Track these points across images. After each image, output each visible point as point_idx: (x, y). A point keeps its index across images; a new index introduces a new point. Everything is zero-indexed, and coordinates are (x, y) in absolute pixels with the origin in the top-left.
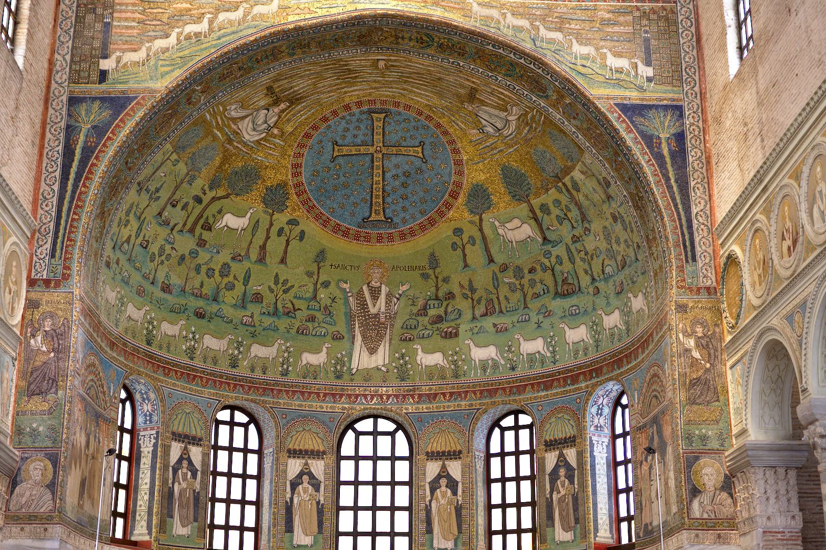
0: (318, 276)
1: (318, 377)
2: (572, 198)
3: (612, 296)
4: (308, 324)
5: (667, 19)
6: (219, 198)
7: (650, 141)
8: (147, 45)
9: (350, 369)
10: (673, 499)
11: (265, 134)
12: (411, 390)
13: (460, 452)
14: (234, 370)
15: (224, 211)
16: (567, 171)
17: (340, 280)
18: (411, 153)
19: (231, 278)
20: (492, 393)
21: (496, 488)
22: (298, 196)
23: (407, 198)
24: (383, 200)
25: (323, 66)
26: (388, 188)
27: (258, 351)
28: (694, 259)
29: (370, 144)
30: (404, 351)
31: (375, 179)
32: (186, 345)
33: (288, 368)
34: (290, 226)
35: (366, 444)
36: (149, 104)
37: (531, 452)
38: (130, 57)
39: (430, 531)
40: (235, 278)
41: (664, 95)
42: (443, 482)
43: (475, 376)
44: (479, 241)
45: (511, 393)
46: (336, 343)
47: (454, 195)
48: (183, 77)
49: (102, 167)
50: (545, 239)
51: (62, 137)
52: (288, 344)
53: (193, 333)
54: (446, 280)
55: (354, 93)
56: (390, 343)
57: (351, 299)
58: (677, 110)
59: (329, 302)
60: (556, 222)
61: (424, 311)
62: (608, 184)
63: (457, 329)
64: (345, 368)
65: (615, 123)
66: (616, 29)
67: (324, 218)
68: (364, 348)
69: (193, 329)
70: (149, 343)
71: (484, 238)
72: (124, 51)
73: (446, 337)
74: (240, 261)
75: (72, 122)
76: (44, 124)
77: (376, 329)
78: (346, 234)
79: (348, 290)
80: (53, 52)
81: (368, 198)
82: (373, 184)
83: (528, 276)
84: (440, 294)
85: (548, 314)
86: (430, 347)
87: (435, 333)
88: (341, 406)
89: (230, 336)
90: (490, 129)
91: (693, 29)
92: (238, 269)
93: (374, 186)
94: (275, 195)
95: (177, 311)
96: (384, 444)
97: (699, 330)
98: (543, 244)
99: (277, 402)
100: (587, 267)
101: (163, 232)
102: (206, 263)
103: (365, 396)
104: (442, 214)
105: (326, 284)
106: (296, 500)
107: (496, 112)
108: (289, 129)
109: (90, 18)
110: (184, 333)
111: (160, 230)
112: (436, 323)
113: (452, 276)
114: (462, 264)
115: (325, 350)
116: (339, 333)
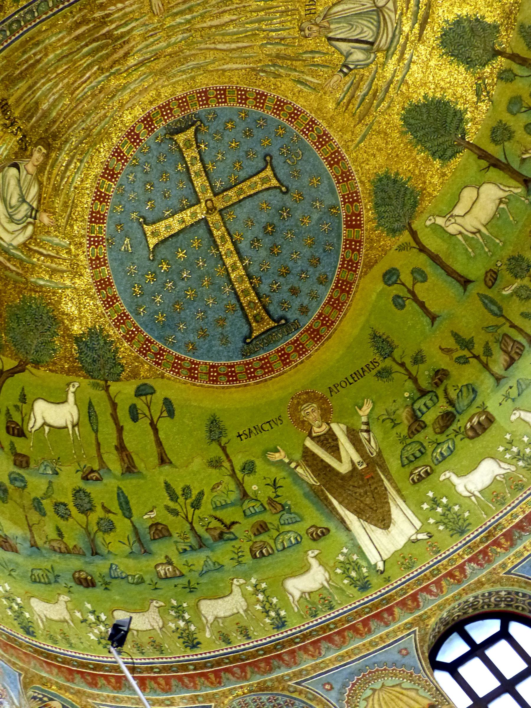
0: (230, 461)
1: (334, 603)
4: (261, 538)
11: (30, 228)
12: (487, 538)
14: (198, 651)
15: (29, 396)
17: (265, 453)
18: (259, 188)
19: (99, 513)
22: (130, 340)
23: (288, 272)
24: (257, 294)
25: (71, 29)
29: (193, 201)
30: (431, 494)
31: (229, 262)
32: (94, 634)
33: (278, 614)
34: (143, 398)
40: (103, 507)
44: (429, 268)
46: (322, 543)
52: (253, 581)
53: (93, 612)
54: (419, 359)
56: (402, 497)
57: (299, 470)
59: (270, 492)
63: (484, 411)
64: (364, 570)
67: (187, 365)
68: (370, 528)
69: (89, 606)
70: (28, 631)
71: (435, 259)
73: (478, 435)
74: (97, 479)
77: (366, 493)
79: (287, 460)
81: (234, 301)
82: (228, 275)
84: (424, 384)
86: (465, 463)
87: (457, 440)
89: (154, 603)
90: (358, 56)
93: (233, 276)
94: (93, 349)
99: (301, 671)
102: (46, 496)
103: (426, 589)
110: (78, 615)
112: (447, 427)
113: (424, 347)
114: (426, 320)
115: (314, 562)
116: (318, 528)
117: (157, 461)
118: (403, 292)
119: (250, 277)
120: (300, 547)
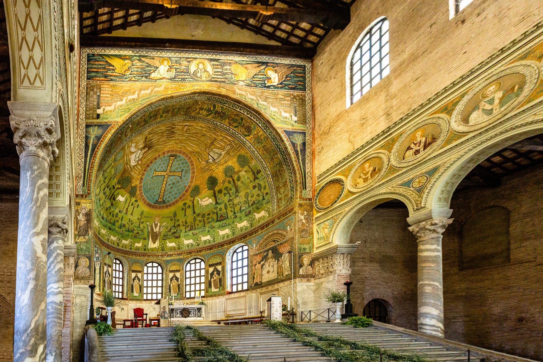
7: (294, 145)
8: (114, 104)
28: (306, 189)
38: (108, 108)
41: (300, 128)
48: (129, 117)
51: (84, 140)
58: (305, 133)
66: (285, 102)
72: (106, 106)
75: (88, 135)
97: (305, 213)
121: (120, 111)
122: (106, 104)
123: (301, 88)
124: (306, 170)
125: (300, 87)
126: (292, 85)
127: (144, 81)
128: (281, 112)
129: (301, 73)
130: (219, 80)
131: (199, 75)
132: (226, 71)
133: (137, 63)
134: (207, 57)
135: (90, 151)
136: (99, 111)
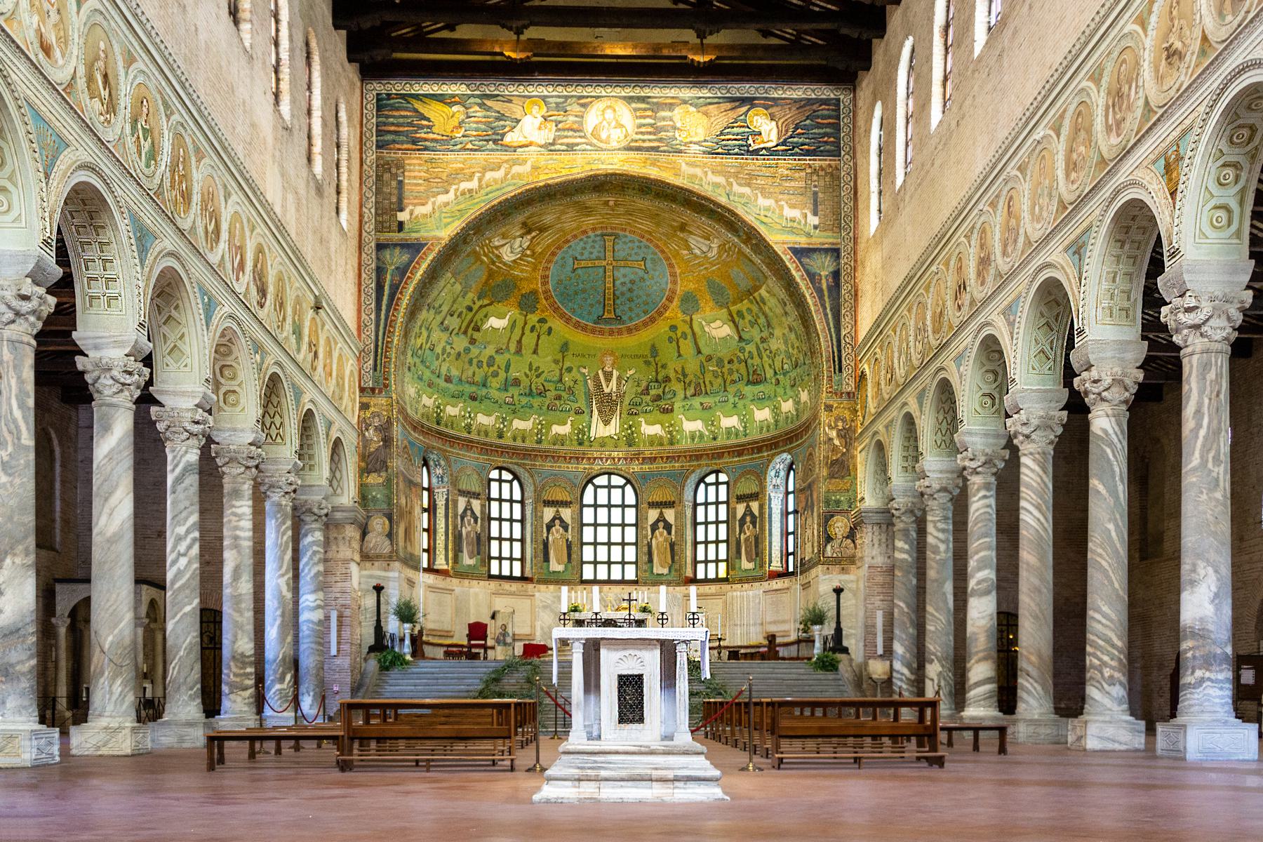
2: (761, 309)
3: (788, 387)
5: (832, 175)
6: (485, 306)
9: (589, 437)
10: (816, 544)
13: (674, 502)
16: (757, 288)
19: (495, 368)
20: (698, 457)
21: (701, 529)
22: (546, 300)
26: (617, 293)
27: (518, 424)
28: (840, 371)
35: (603, 494)
36: (437, 249)
37: (727, 503)
38: (420, 210)
39: (650, 560)
40: (499, 367)
41: (826, 240)
42: (661, 524)
43: (685, 444)
44: (689, 337)
45: (713, 458)
47: (670, 300)
49: (405, 301)
50: (740, 337)
51: (374, 276)
54: (664, 366)
55: (590, 221)
59: (572, 384)
60: (748, 326)
61: (646, 391)
62: (785, 305)
65: (787, 263)
66: (793, 184)
71: (694, 334)
72: (415, 205)
75: (381, 265)
76: (360, 265)
78: (584, 329)
80: (361, 207)
83: (727, 366)
84: (660, 378)
85: (742, 397)
88: (584, 465)
91: (852, 184)
92: (501, 360)
95: (456, 396)
96: (616, 494)
98: (739, 341)
100: (771, 362)
101: (445, 336)
102: (477, 357)
103: (601, 459)
104: (660, 314)
105: (569, 370)
106: (550, 539)
107: (702, 240)
108: (539, 250)
109: (387, 176)
111: (442, 334)
114: (676, 354)
115: (569, 422)
117: (532, 351)
118: (674, 337)
119: (614, 294)
120: (567, 414)
121: (443, 215)
122: (416, 201)
123: (828, 151)
124: (843, 330)
125: (828, 147)
126: (808, 145)
127: (492, 150)
128: (781, 208)
129: (830, 117)
130: (647, 144)
131: (604, 136)
132: (665, 123)
133: (476, 112)
134: (623, 94)
135: (385, 298)
136: (402, 216)
